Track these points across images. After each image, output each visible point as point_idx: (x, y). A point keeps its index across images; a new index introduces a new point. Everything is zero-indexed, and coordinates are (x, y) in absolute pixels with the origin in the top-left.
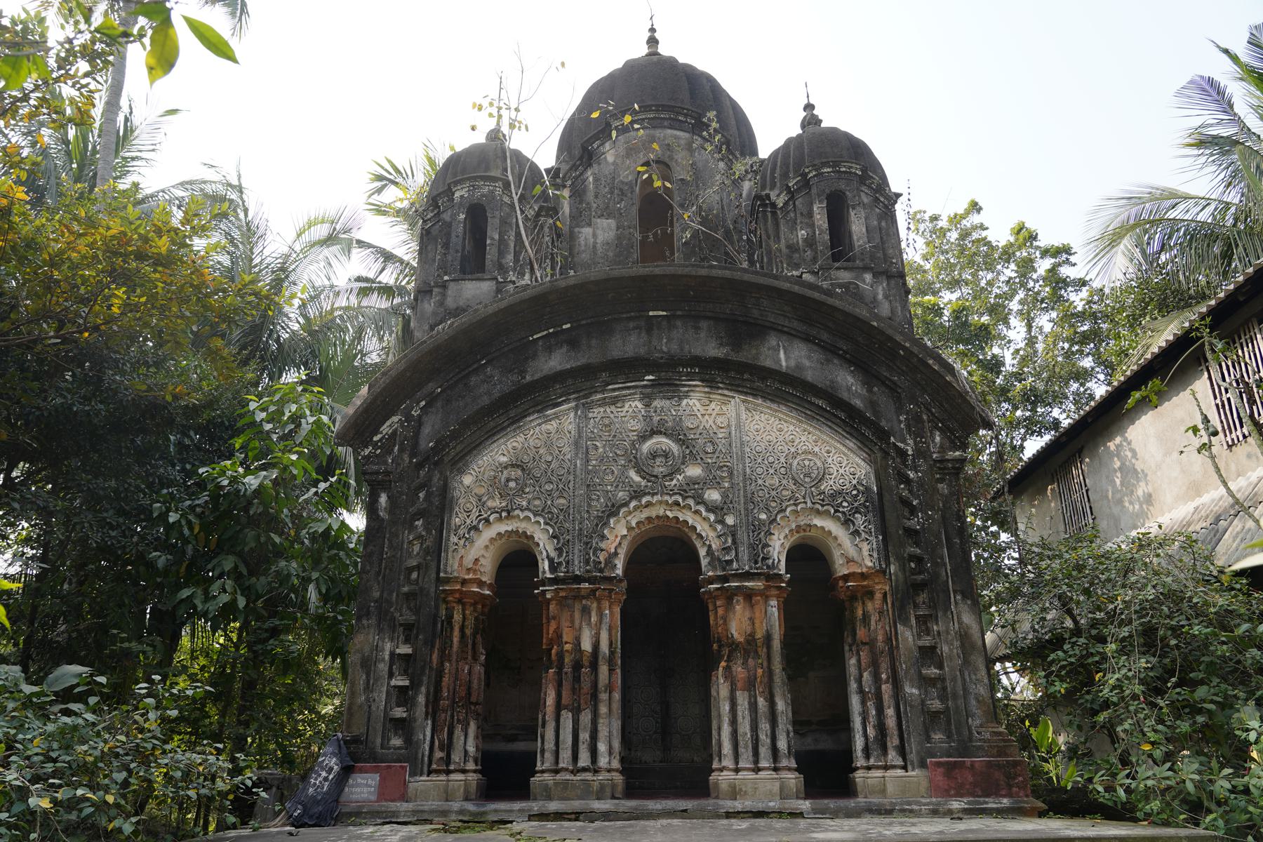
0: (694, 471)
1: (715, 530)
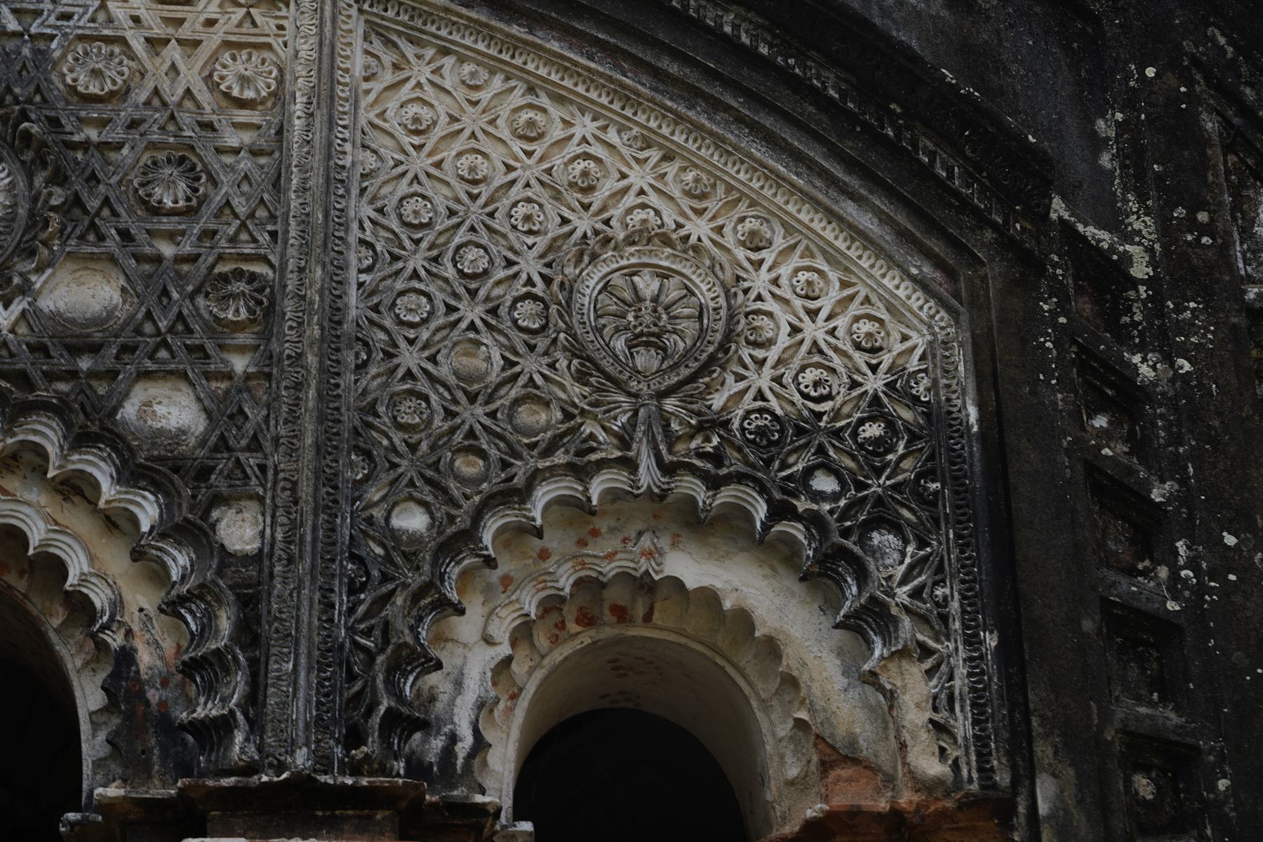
0: (82, 292)
1: (159, 575)
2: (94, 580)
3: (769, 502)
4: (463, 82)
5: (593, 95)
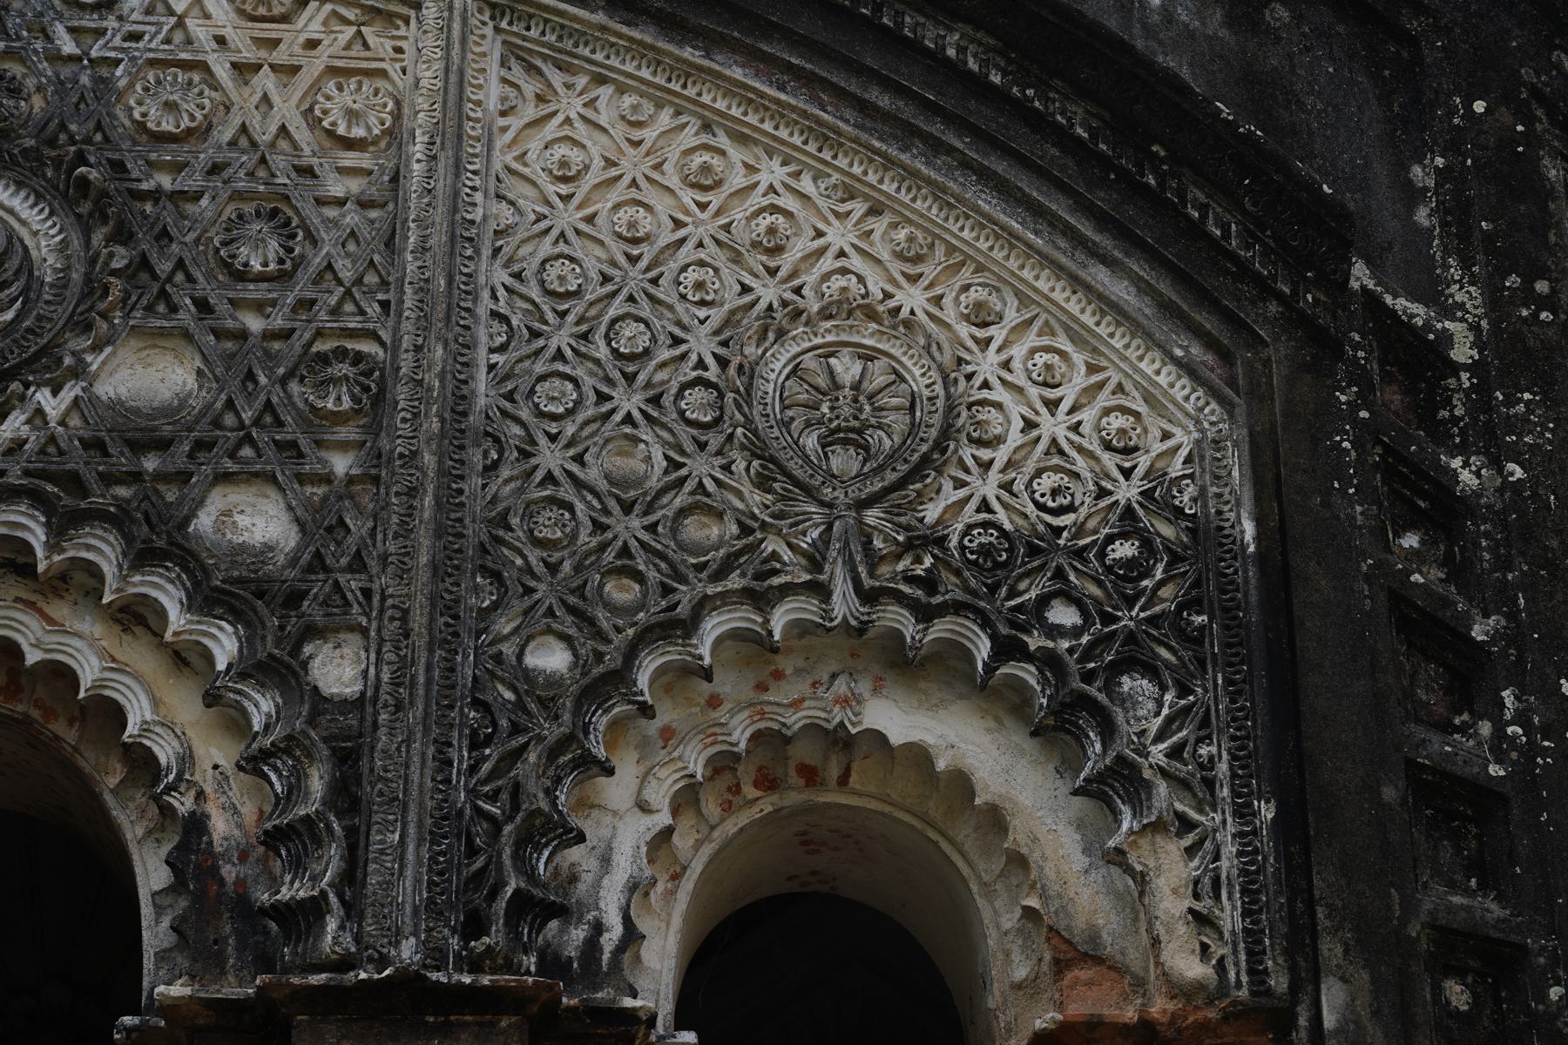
0: (149, 376)
1: (237, 724)
2: (158, 729)
3: (994, 638)
4: (623, 118)
5: (783, 133)
